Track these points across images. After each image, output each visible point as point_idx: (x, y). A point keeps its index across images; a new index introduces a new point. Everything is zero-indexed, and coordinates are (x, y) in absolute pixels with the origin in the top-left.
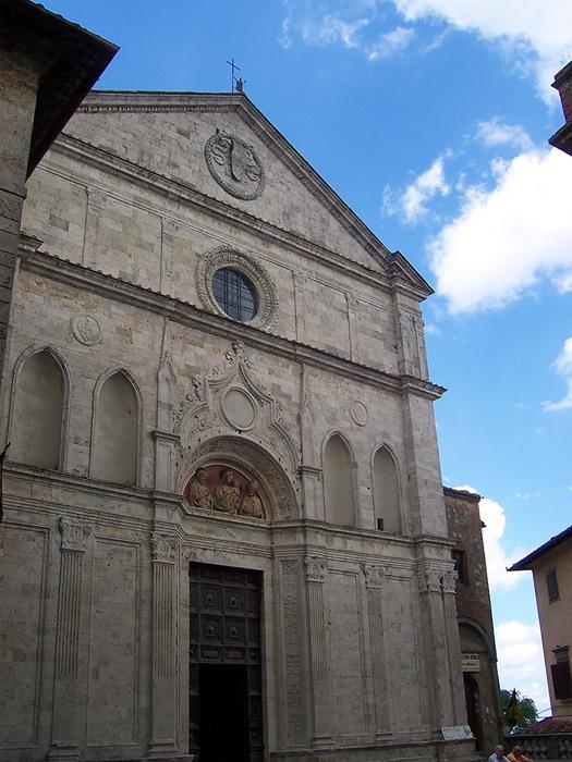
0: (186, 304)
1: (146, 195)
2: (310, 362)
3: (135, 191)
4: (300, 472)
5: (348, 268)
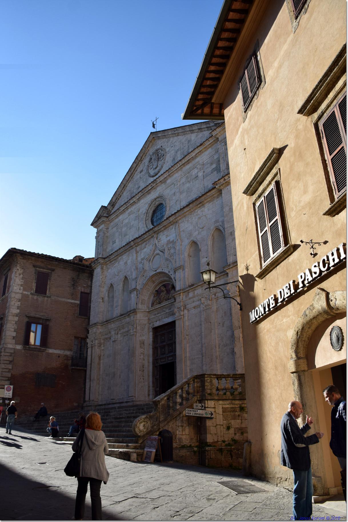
0: (135, 239)
1: (129, 210)
2: (178, 219)
3: (127, 212)
4: (175, 272)
5: (194, 155)
